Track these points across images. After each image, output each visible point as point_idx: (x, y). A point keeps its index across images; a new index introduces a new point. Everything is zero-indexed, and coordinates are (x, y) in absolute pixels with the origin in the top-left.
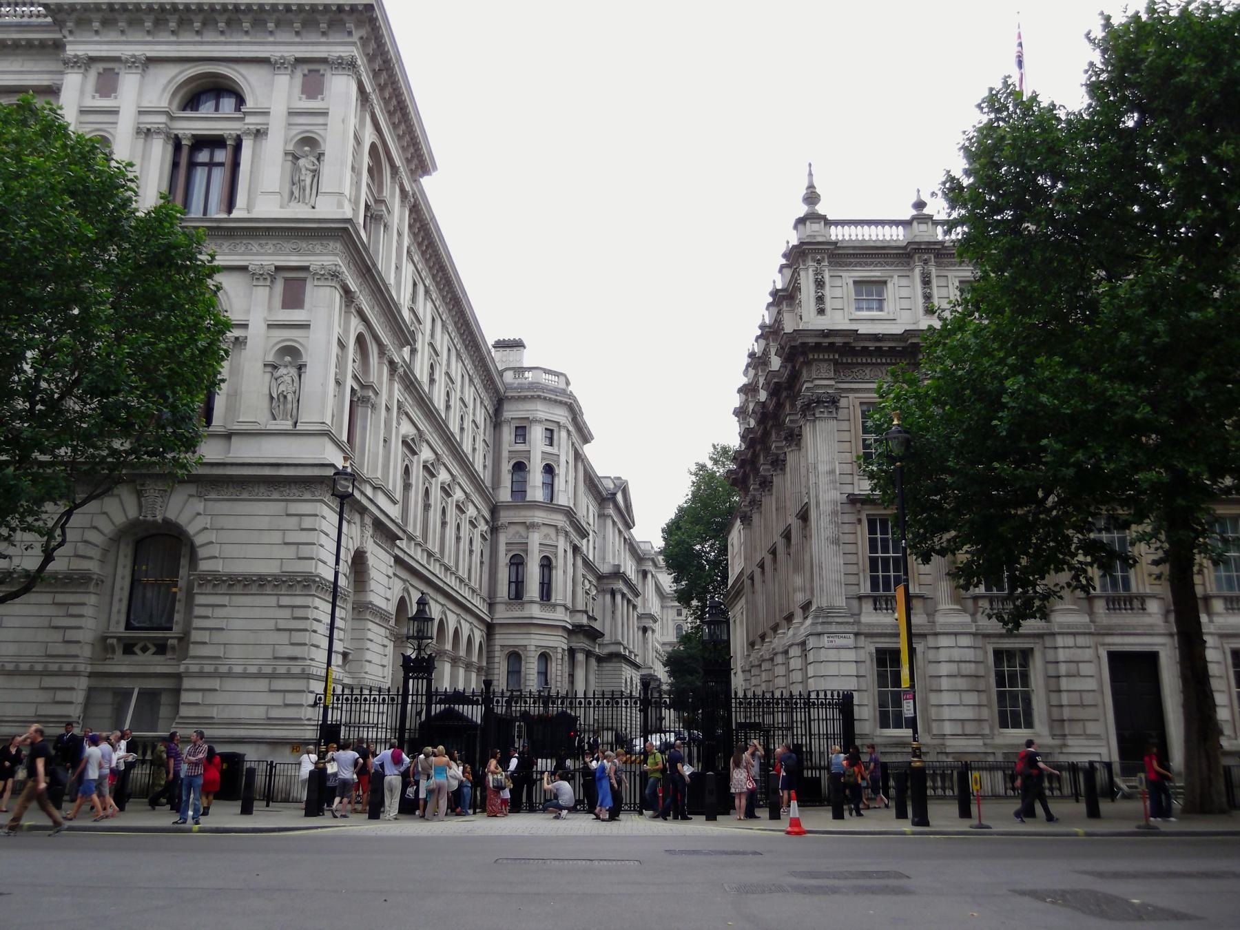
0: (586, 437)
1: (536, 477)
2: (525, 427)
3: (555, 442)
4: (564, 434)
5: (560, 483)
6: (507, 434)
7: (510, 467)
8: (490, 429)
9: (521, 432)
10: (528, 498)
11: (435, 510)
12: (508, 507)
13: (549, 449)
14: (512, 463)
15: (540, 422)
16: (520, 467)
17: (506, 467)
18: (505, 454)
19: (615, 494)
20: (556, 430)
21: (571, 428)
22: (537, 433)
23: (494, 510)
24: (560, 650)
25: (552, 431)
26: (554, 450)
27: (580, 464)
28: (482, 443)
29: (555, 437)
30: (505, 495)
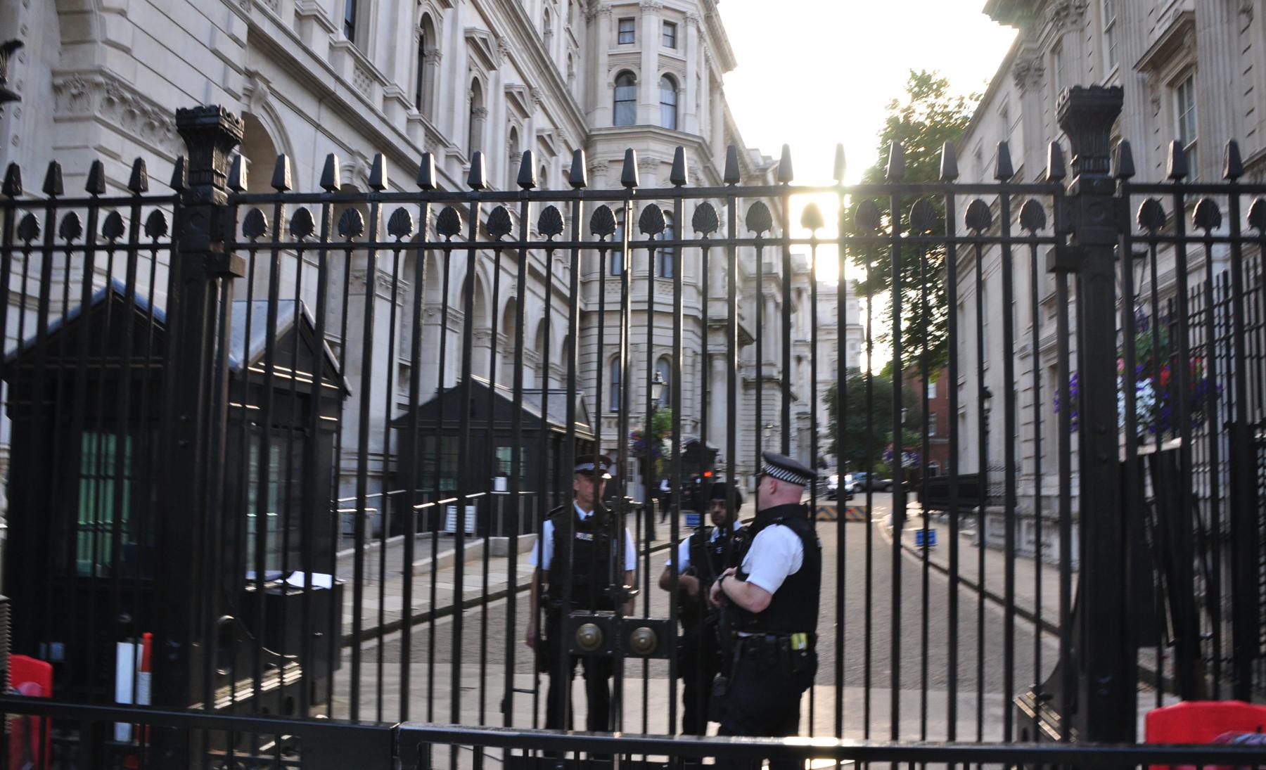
0: (727, 63)
1: (651, 91)
2: (632, 19)
3: (680, 43)
4: (692, 30)
5: (688, 102)
6: (606, 30)
7: (611, 78)
8: (578, 25)
9: (627, 25)
10: (639, 123)
11: (453, 70)
12: (608, 137)
13: (670, 52)
14: (615, 71)
15: (657, 9)
16: (626, 78)
17: (605, 79)
18: (603, 59)
19: (764, 170)
20: (680, 23)
21: (703, 28)
22: (651, 27)
23: (588, 141)
24: (689, 353)
25: (673, 25)
26: (678, 54)
27: (717, 97)
28: (564, 36)
29: (680, 35)
30: (603, 119)
